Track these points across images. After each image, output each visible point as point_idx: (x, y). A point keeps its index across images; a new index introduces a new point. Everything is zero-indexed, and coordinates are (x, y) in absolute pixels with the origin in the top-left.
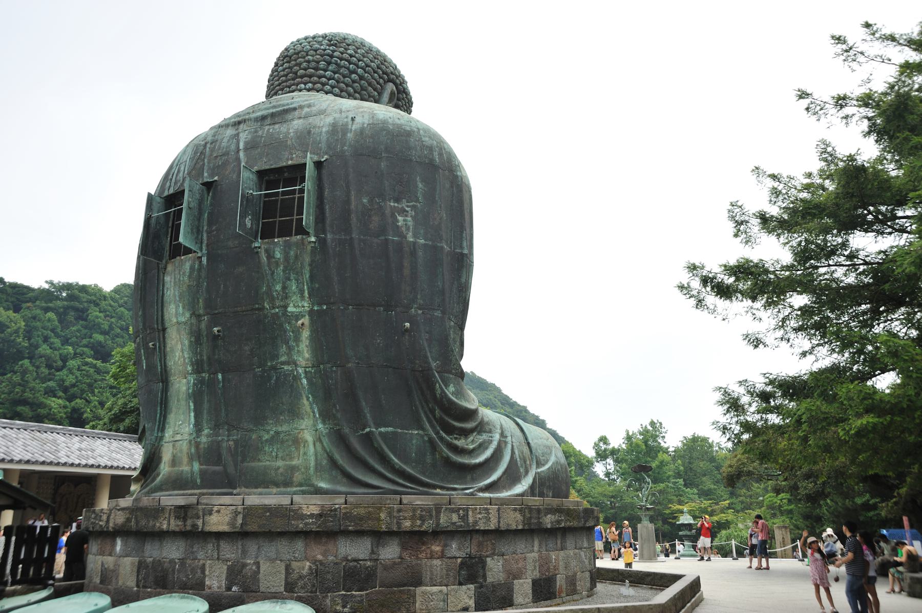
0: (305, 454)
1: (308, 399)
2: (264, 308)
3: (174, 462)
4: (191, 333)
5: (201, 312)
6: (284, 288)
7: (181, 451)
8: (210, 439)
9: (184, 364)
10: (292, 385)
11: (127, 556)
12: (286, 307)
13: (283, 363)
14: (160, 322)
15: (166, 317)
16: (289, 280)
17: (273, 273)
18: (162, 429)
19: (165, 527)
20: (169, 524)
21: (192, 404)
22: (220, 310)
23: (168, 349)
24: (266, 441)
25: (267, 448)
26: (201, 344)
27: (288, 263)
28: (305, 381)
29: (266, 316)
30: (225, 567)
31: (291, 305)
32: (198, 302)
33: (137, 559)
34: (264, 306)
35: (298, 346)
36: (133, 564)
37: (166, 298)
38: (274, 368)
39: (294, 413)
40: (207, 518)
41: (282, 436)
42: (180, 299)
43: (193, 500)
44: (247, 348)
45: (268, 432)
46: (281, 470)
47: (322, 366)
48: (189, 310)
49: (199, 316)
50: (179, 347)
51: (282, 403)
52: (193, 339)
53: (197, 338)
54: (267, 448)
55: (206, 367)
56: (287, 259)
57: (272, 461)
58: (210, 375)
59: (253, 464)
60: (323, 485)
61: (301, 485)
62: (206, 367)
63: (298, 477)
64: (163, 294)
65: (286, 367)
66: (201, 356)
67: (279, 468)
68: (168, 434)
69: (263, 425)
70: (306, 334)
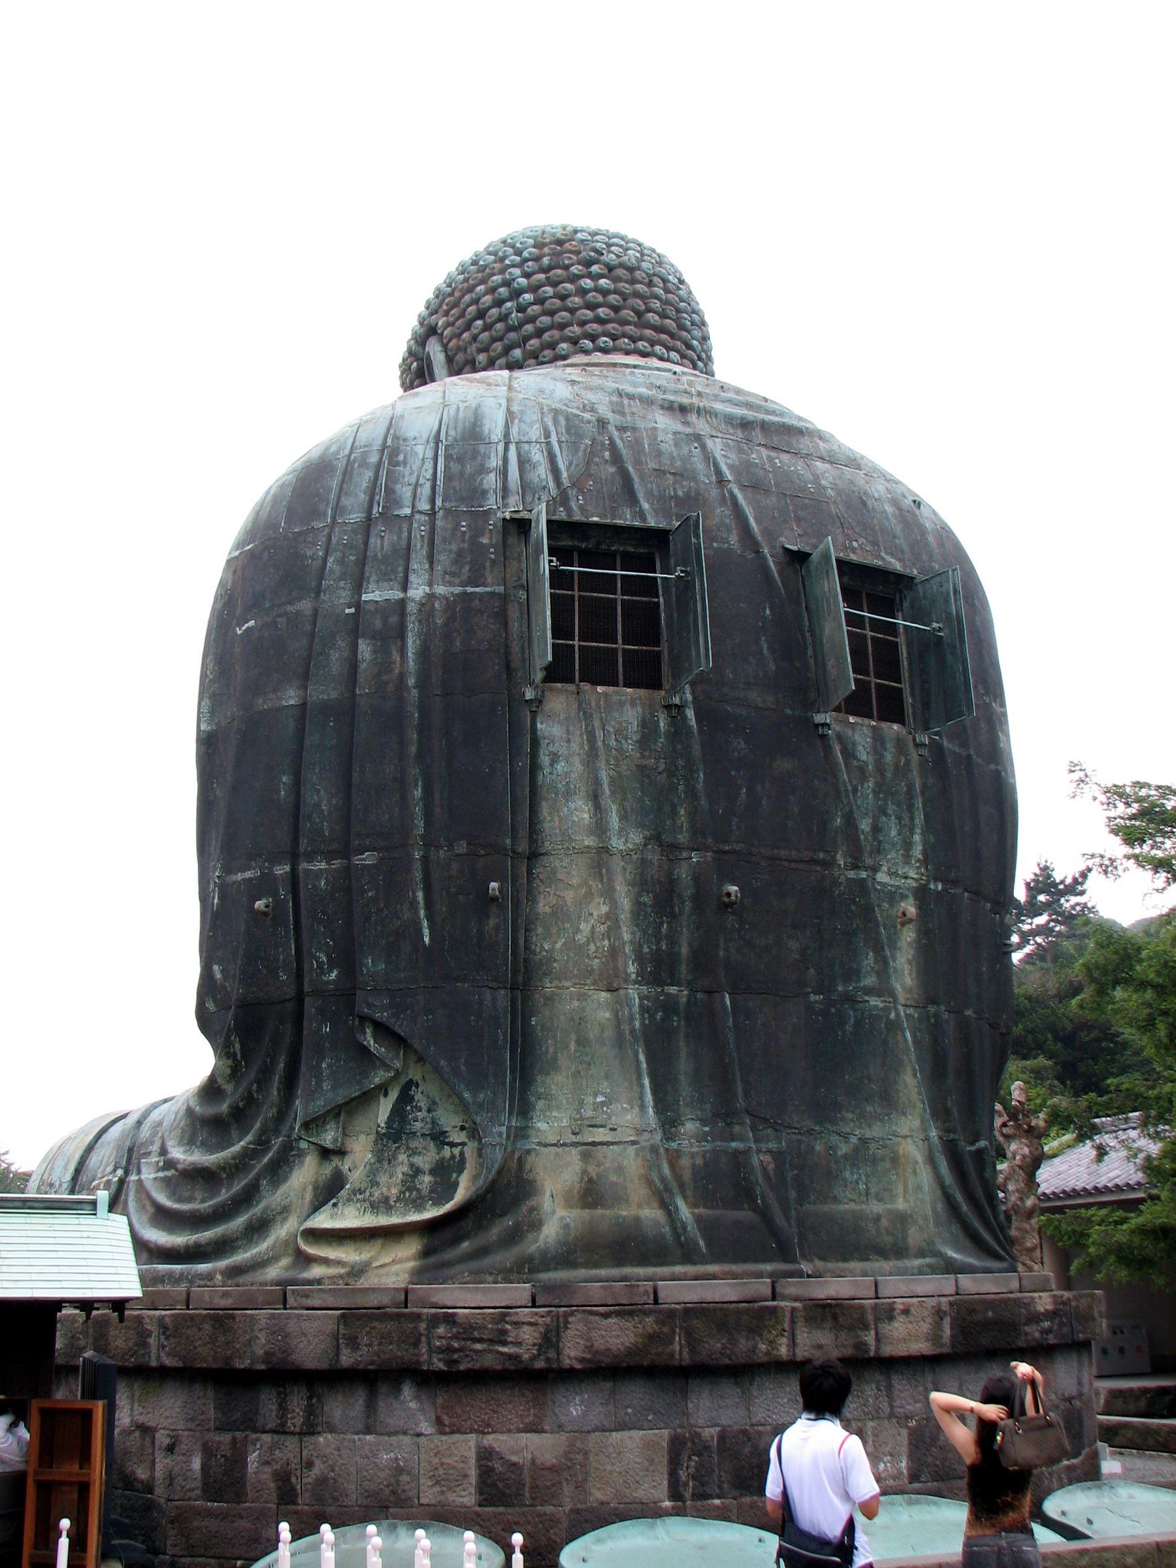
0: (919, 1188)
1: (915, 1075)
2: (832, 863)
3: (591, 1194)
4: (641, 883)
5: (683, 838)
6: (876, 829)
7: (620, 1169)
8: (708, 1147)
9: (614, 952)
10: (885, 1042)
11: (622, 1427)
12: (875, 869)
13: (869, 991)
14: (523, 833)
15: (550, 823)
16: (885, 814)
17: (855, 790)
18: (524, 1110)
19: (783, 1351)
20: (793, 1343)
21: (642, 1057)
22: (738, 847)
23: (543, 906)
24: (845, 1156)
25: (847, 1174)
26: (673, 916)
27: (882, 775)
28: (908, 1035)
29: (835, 883)
30: (904, 1432)
31: (885, 869)
32: (674, 813)
33: (666, 1433)
34: (834, 859)
35: (894, 961)
36: (648, 1445)
37: (546, 776)
38: (850, 999)
39: (889, 1101)
40: (885, 1328)
41: (872, 1146)
42: (613, 792)
43: (762, 1287)
44: (794, 945)
45: (845, 1137)
46: (884, 1222)
47: (932, 1009)
48: (641, 826)
49: (675, 847)
50: (601, 908)
51: (870, 1080)
52: (646, 899)
53: (659, 899)
54: (847, 1174)
55: (683, 971)
56: (880, 768)
57: (857, 1200)
58: (693, 991)
59: (827, 1208)
60: (951, 1253)
61: (922, 1254)
62: (683, 971)
63: (914, 1237)
64: (535, 767)
65: (874, 1001)
66: (673, 942)
67: (878, 1218)
68: (549, 1124)
69: (834, 1122)
70: (908, 935)
